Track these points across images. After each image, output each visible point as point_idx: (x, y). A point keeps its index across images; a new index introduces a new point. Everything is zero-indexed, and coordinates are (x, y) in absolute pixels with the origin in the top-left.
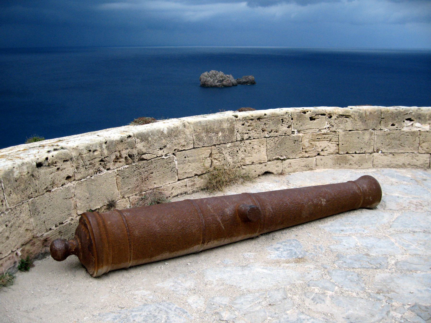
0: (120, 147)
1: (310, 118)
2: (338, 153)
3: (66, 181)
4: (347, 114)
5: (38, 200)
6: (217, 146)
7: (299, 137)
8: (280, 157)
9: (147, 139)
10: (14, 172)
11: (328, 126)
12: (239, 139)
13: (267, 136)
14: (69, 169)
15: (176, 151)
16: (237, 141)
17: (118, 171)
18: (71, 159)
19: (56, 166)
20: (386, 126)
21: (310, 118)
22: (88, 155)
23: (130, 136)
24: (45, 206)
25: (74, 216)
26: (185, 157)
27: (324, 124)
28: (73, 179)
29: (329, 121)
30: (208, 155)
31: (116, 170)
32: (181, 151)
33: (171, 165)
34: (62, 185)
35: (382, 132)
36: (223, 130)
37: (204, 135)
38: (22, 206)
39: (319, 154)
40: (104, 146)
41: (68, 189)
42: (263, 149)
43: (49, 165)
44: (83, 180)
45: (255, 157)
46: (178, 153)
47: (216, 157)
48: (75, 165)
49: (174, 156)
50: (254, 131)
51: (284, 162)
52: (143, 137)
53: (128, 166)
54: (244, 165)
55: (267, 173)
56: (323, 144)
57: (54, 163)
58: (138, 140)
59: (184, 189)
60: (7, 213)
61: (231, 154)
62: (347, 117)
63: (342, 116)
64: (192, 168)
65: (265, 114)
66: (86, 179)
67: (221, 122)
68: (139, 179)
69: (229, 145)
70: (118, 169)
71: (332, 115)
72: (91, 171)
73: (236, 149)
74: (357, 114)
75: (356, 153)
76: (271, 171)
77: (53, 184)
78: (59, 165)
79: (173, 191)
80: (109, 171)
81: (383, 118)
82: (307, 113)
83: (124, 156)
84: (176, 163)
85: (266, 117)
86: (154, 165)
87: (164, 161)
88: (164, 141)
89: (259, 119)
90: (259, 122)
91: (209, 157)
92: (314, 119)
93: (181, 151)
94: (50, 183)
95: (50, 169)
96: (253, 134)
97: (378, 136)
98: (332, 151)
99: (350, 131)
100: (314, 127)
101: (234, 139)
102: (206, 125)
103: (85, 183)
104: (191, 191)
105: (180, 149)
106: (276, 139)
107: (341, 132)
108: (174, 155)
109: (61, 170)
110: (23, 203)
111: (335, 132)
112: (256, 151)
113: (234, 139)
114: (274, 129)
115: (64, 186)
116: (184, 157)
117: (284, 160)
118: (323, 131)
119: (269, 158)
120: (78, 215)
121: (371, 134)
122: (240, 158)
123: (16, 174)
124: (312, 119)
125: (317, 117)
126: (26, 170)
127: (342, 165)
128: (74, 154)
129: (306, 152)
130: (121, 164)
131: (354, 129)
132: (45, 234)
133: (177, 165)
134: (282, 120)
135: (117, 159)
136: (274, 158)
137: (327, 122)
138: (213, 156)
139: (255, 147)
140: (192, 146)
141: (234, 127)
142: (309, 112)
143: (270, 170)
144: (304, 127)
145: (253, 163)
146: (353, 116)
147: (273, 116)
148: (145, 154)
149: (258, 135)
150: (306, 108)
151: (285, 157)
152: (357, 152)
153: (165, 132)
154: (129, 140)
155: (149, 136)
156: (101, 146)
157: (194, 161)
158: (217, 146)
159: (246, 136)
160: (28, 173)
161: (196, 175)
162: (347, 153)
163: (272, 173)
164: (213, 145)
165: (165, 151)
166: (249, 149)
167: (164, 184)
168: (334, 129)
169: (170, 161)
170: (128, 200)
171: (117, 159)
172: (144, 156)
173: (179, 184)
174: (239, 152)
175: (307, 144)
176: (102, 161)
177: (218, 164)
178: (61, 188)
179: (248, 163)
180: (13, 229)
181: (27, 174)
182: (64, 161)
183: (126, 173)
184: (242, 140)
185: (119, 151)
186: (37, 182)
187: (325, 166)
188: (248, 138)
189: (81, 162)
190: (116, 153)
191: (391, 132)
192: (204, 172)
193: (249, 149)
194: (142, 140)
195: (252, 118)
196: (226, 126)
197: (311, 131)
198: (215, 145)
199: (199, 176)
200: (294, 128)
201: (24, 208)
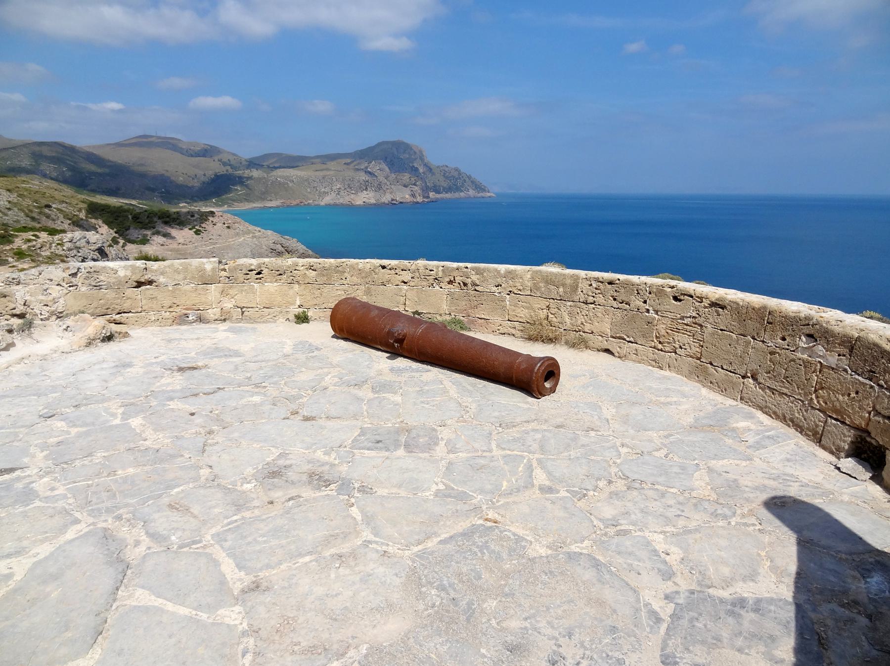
0: (455, 273)
2: (699, 359)
11: (694, 314)
14: (406, 276)
20: (772, 338)
27: (688, 309)
33: (503, 304)
36: (564, 285)
37: (542, 285)
42: (607, 320)
45: (596, 326)
52: (478, 272)
55: (607, 351)
56: (684, 339)
61: (570, 313)
62: (723, 307)
64: (523, 314)
69: (569, 304)
77: (389, 281)
78: (397, 271)
81: (771, 323)
89: (610, 283)
90: (609, 286)
92: (680, 300)
96: (600, 299)
99: (722, 330)
107: (709, 328)
111: (701, 326)
113: (576, 298)
114: (626, 299)
122: (579, 322)
124: (676, 299)
127: (701, 378)
129: (660, 342)
139: (600, 315)
141: (577, 286)
145: (592, 333)
151: (632, 339)
152: (725, 367)
159: (591, 299)
162: (711, 364)
168: (700, 320)
172: (477, 288)
175: (663, 332)
187: (679, 372)
191: (778, 350)
195: (601, 280)
196: (568, 281)
200: (650, 306)
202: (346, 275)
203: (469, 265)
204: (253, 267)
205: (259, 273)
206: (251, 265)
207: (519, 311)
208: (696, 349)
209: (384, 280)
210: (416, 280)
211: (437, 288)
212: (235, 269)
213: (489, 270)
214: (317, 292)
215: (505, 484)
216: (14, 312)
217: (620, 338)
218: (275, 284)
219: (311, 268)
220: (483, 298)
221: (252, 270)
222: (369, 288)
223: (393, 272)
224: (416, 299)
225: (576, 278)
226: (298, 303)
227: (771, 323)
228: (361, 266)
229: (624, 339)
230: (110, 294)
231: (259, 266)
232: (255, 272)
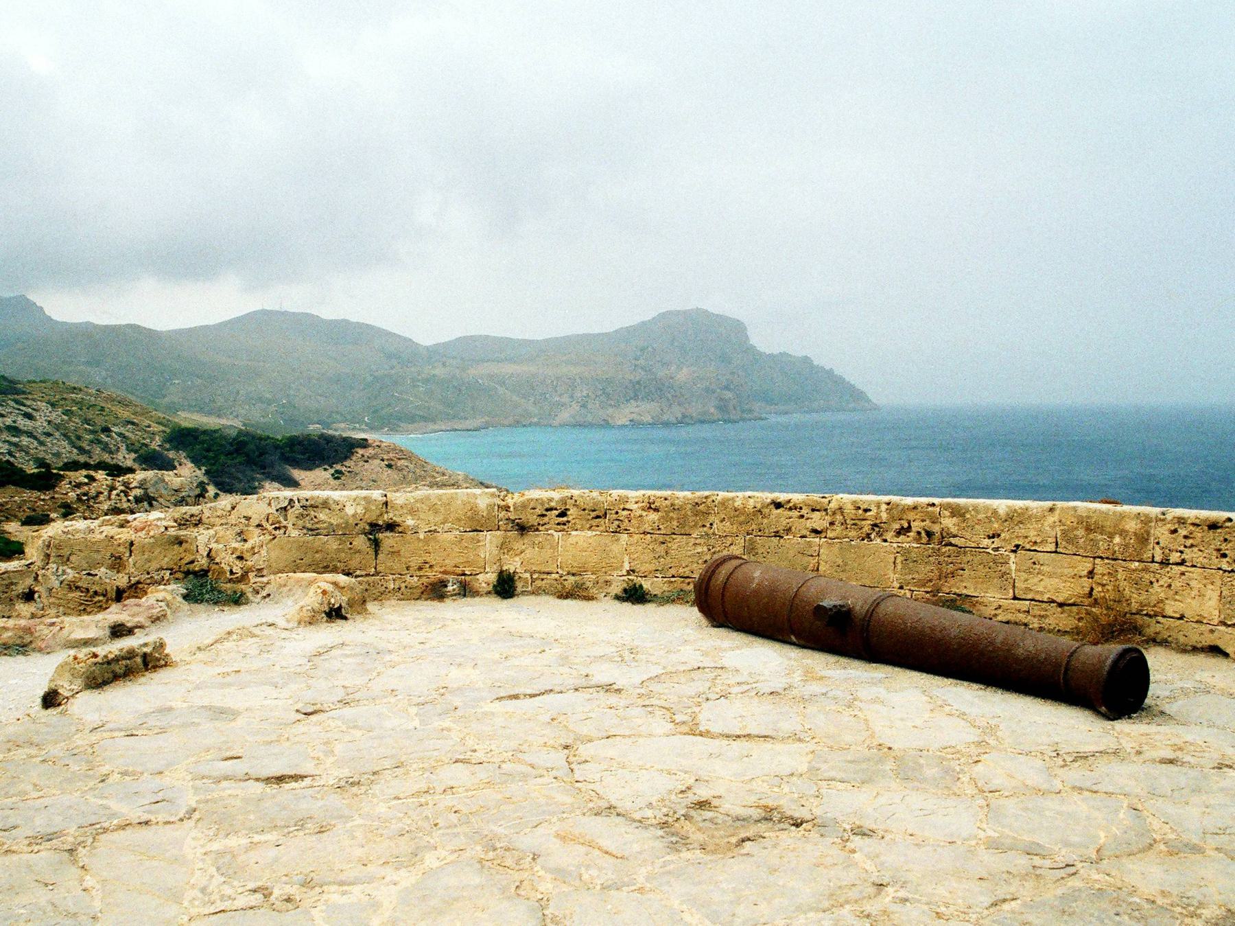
0: (911, 515)
9: (963, 515)
12: (1157, 559)
13: (1225, 567)
14: (818, 521)
16: (1153, 562)
18: (826, 510)
28: (823, 535)
30: (1085, 573)
33: (1003, 569)
36: (1123, 533)
37: (1081, 532)
40: (884, 507)
41: (810, 545)
42: (1212, 594)
43: (790, 509)
45: (1189, 605)
48: (828, 518)
50: (1195, 549)
52: (956, 512)
54: (1164, 617)
58: (947, 513)
67: (1122, 516)
72: (853, 533)
73: (1148, 577)
76: (1222, 647)
77: (788, 531)
78: (804, 512)
79: (999, 611)
84: (1013, 567)
85: (1228, 524)
86: (969, 557)
88: (996, 525)
89: (1213, 526)
101: (1147, 556)
102: (1088, 517)
105: (1028, 547)
112: (1193, 593)
139: (1193, 583)
140: (1052, 547)
141: (1148, 533)
145: (1182, 618)
148: (955, 536)
149: (1206, 561)
154: (930, 509)
155: (968, 511)
156: (879, 507)
159: (1175, 557)
163: (1226, 655)
166: (1177, 584)
171: (902, 531)
172: (953, 540)
174: (1155, 585)
179: (1169, 612)
182: (813, 510)
183: (913, 555)
184: (1165, 563)
186: (765, 521)
188: (1179, 560)
189: (839, 517)
193: (1179, 584)
194: (953, 515)
195: (1197, 521)
196: (1132, 526)
198: (1101, 558)
202: (711, 518)
203: (936, 501)
204: (553, 504)
205: (563, 514)
206: (551, 500)
207: (1036, 580)
209: (780, 528)
210: (838, 529)
211: (879, 540)
212: (524, 506)
213: (976, 509)
214: (661, 549)
215: (1102, 834)
216: (191, 567)
218: (590, 533)
219: (651, 507)
220: (965, 559)
221: (551, 509)
222: (752, 542)
223: (795, 513)
224: (840, 562)
225: (1146, 521)
226: (627, 567)
228: (738, 504)
230: (333, 544)
231: (564, 501)
232: (557, 512)
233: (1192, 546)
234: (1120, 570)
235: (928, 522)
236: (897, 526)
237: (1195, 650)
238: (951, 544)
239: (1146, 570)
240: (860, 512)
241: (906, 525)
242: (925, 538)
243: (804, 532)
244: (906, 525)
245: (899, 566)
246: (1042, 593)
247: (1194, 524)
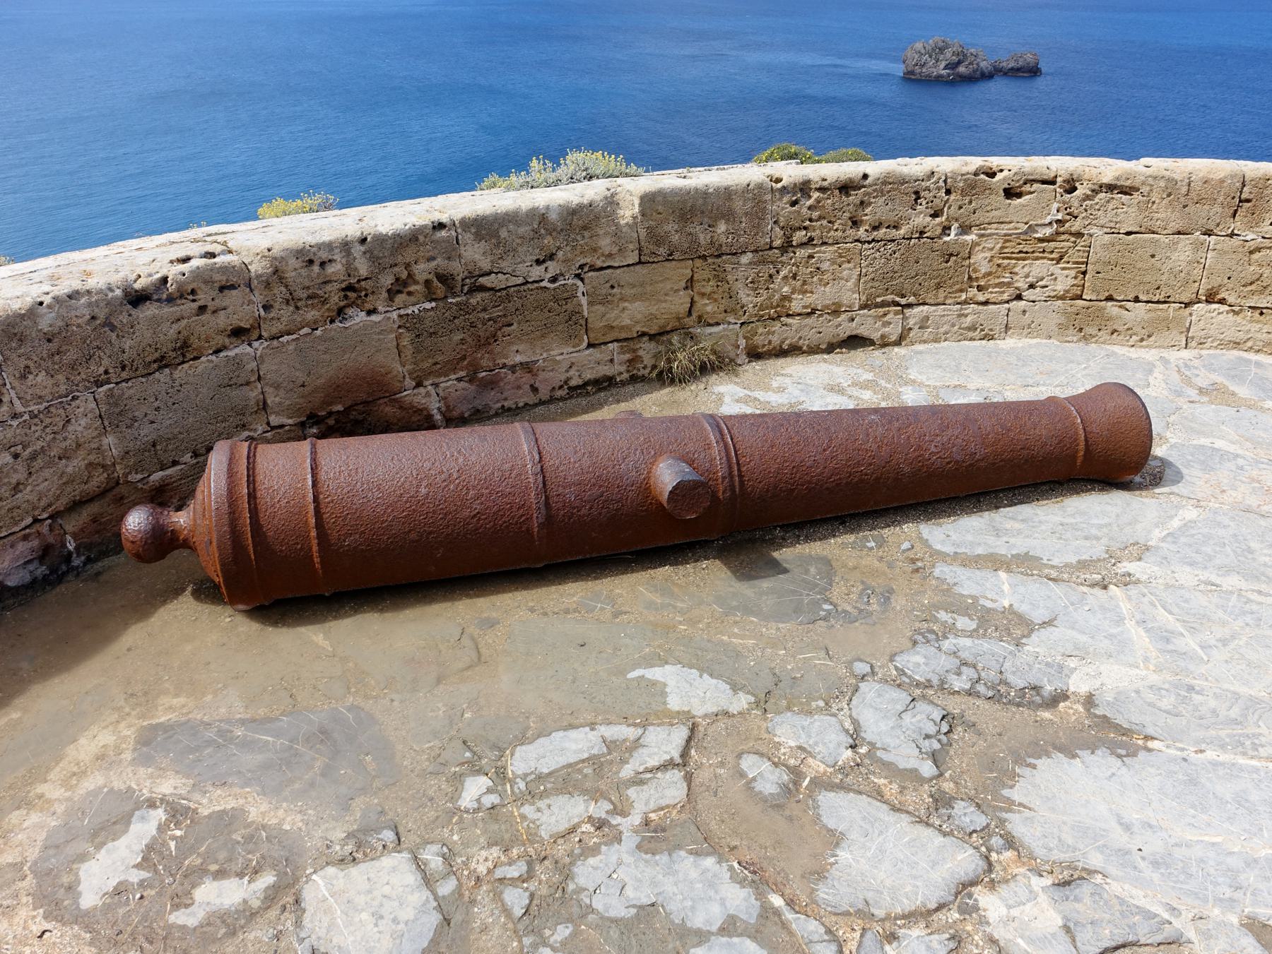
1: (1005, 190)
2: (1080, 297)
3: (227, 341)
4: (1128, 183)
5: (129, 388)
6: (710, 260)
7: (964, 244)
8: (897, 299)
10: (42, 316)
12: (777, 243)
14: (239, 309)
15: (586, 269)
16: (771, 248)
17: (400, 316)
19: (194, 301)
21: (1005, 190)
22: (304, 272)
23: (440, 226)
24: (156, 404)
25: (255, 430)
26: (612, 287)
28: (255, 334)
29: (1064, 203)
30: (683, 284)
31: (395, 315)
32: (602, 269)
33: (570, 307)
34: (217, 352)
35: (1235, 241)
37: (671, 227)
38: (74, 404)
39: (1019, 297)
40: (358, 250)
41: (238, 363)
44: (285, 339)
45: (822, 296)
46: (590, 274)
47: (708, 290)
48: (258, 298)
49: (579, 283)
51: (908, 312)
52: (483, 227)
53: (434, 304)
54: (788, 316)
55: (855, 342)
56: (1039, 268)
57: (186, 293)
58: (467, 237)
59: (607, 370)
60: (15, 423)
63: (1111, 188)
65: (865, 176)
66: (294, 336)
67: (727, 193)
68: (469, 340)
69: (745, 259)
70: (402, 312)
71: (1077, 184)
72: (312, 314)
74: (1162, 184)
75: (1137, 300)
78: (203, 298)
79: (572, 373)
80: (374, 318)
81: (1248, 201)
82: (999, 176)
83: (421, 277)
84: (584, 301)
87: (546, 295)
89: (846, 187)
91: (686, 288)
92: (1019, 195)
93: (602, 269)
94: (170, 346)
95: (175, 309)
97: (1223, 253)
98: (1060, 287)
99: (1129, 233)
100: (1015, 219)
103: (291, 347)
104: (626, 376)
105: (599, 264)
106: (891, 246)
108: (582, 280)
109: (214, 312)
110: (74, 398)
111: (1079, 235)
115: (222, 354)
116: (608, 285)
117: (909, 306)
118: (1048, 231)
119: (864, 298)
120: (273, 428)
121: (1198, 246)
123: (46, 322)
124: (1010, 193)
125: (1027, 188)
126: (87, 313)
128: (256, 268)
129: (980, 288)
130: (412, 299)
131: (1143, 229)
132: (157, 476)
133: (585, 307)
134: (917, 193)
135: (399, 287)
136: (879, 300)
137: (1056, 205)
138: (697, 286)
139: (825, 266)
140: (633, 258)
142: (1006, 173)
143: (863, 331)
144: (980, 217)
146: (1145, 189)
147: (890, 184)
150: (994, 162)
151: (912, 299)
152: (1142, 297)
153: (553, 216)
157: (635, 298)
158: (710, 260)
159: (799, 236)
160: (93, 318)
161: (644, 334)
162: (1110, 298)
164: (699, 257)
165: (553, 268)
166: (804, 271)
167: (545, 355)
168: (1076, 226)
169: (566, 295)
170: (433, 392)
171: (399, 287)
173: (590, 355)
176: (350, 288)
177: (709, 309)
178: (213, 358)
180: (39, 462)
181: (88, 323)
182: (222, 289)
185: (407, 266)
186: (127, 344)
188: (805, 240)
189: (280, 291)
190: (396, 269)
192: (668, 328)
194: (479, 237)
195: (825, 184)
197: (1004, 229)
198: (704, 258)
199: (652, 337)
201: (82, 410)
208: (1064, 280)
217: (884, 304)
223: (189, 307)
227: (1248, 201)
229: (898, 304)
233: (820, 218)
234: (728, 267)
235: (439, 261)
236: (387, 280)
237: (830, 349)
238: (483, 289)
239: (763, 262)
240: (316, 268)
241: (404, 275)
242: (440, 289)
243: (222, 340)
244: (404, 275)
245: (408, 352)
246: (627, 328)
247: (822, 189)
